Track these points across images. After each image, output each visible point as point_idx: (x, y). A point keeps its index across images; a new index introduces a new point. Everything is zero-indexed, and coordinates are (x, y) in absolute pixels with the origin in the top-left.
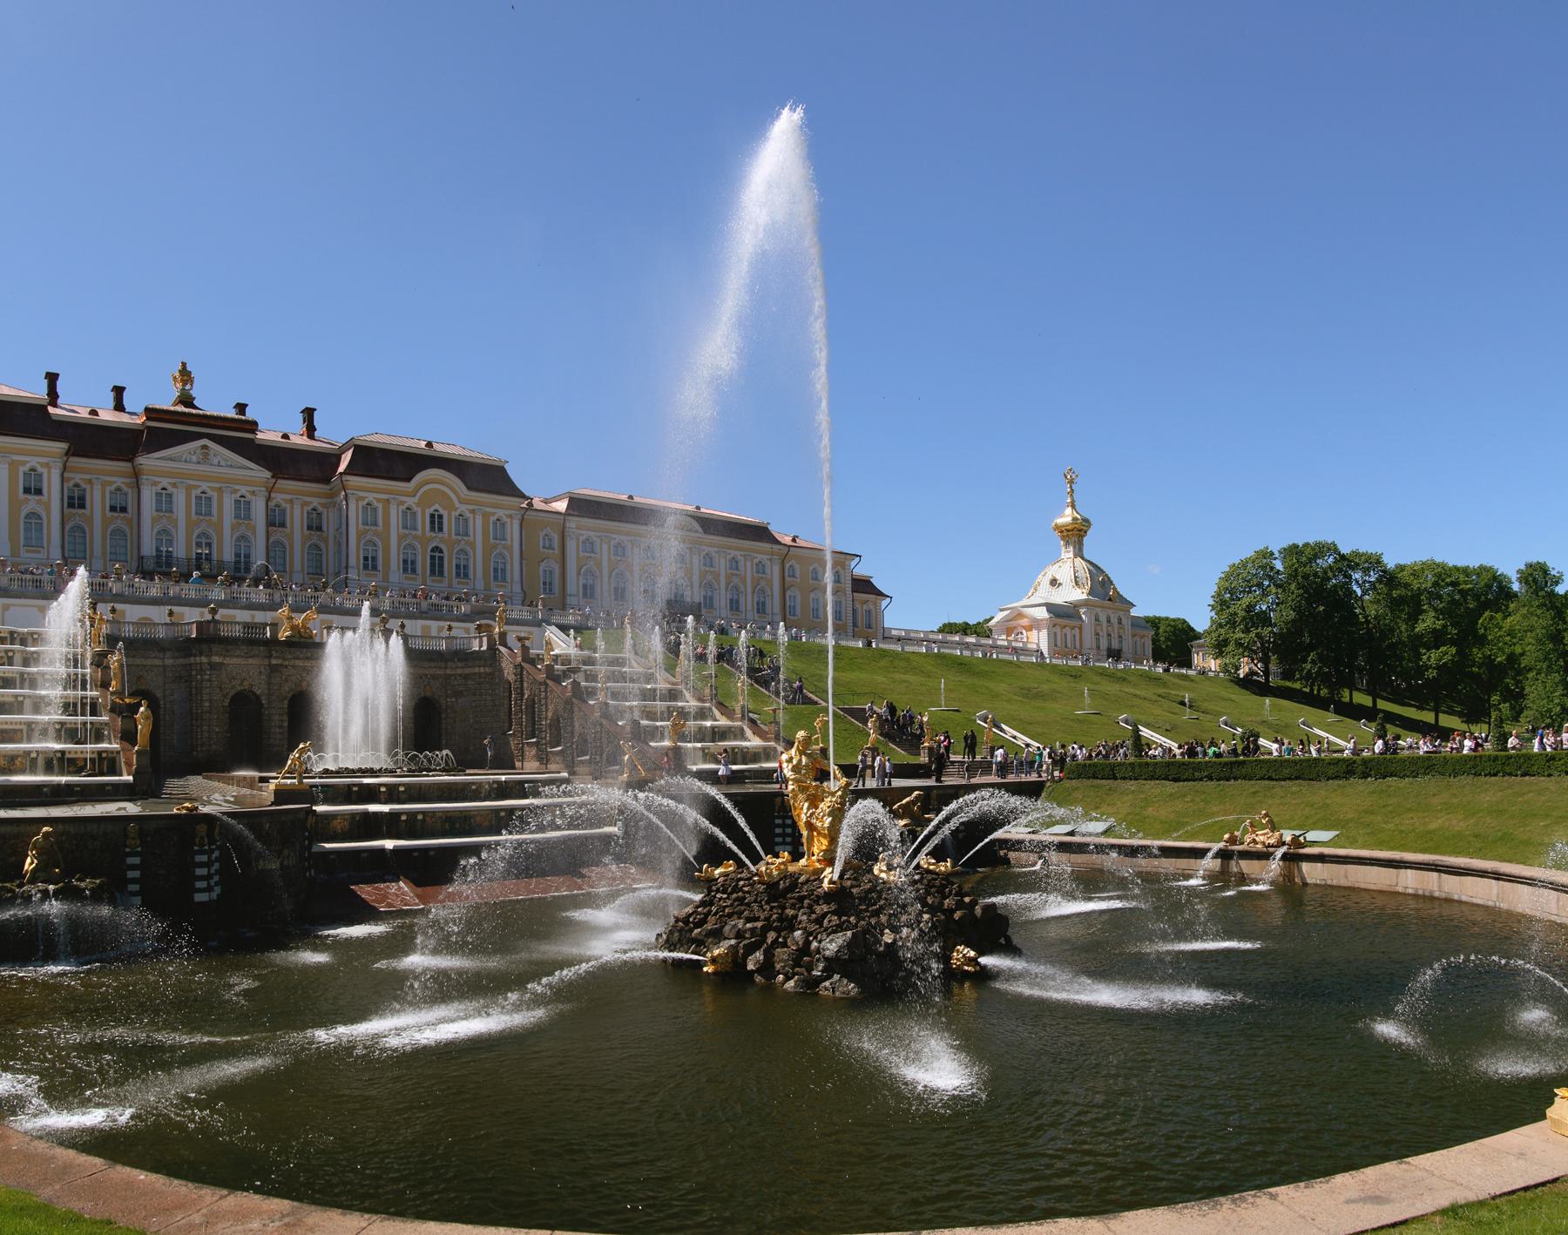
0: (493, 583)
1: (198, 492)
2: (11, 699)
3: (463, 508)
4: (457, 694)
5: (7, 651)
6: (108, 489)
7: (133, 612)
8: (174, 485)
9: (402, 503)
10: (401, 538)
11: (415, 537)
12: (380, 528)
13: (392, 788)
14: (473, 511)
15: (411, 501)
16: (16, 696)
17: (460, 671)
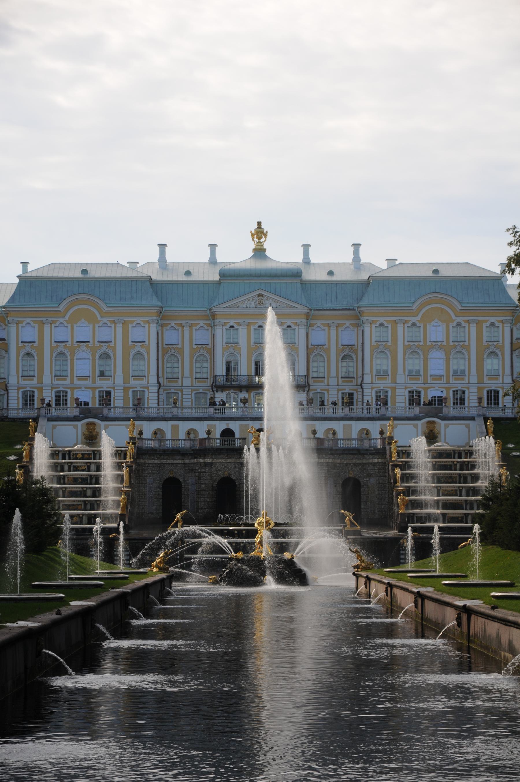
0: (486, 380)
1: (256, 326)
2: (81, 489)
3: (459, 320)
4: (369, 476)
5: (87, 463)
6: (194, 329)
7: (184, 427)
8: (238, 324)
9: (406, 322)
10: (406, 348)
11: (418, 347)
12: (390, 343)
13: (240, 531)
14: (468, 322)
15: (414, 320)
16: (83, 488)
17: (371, 461)
